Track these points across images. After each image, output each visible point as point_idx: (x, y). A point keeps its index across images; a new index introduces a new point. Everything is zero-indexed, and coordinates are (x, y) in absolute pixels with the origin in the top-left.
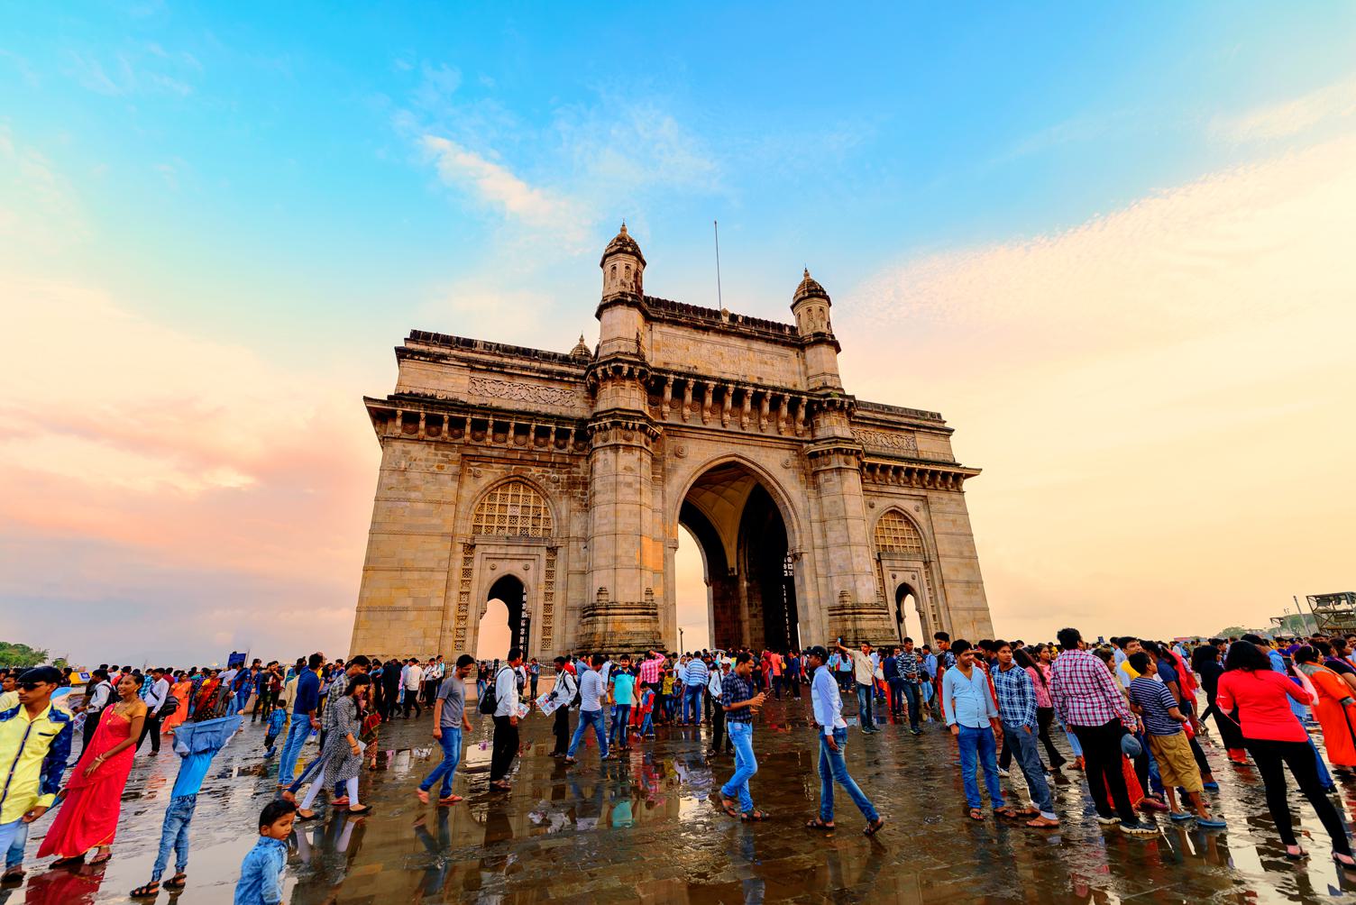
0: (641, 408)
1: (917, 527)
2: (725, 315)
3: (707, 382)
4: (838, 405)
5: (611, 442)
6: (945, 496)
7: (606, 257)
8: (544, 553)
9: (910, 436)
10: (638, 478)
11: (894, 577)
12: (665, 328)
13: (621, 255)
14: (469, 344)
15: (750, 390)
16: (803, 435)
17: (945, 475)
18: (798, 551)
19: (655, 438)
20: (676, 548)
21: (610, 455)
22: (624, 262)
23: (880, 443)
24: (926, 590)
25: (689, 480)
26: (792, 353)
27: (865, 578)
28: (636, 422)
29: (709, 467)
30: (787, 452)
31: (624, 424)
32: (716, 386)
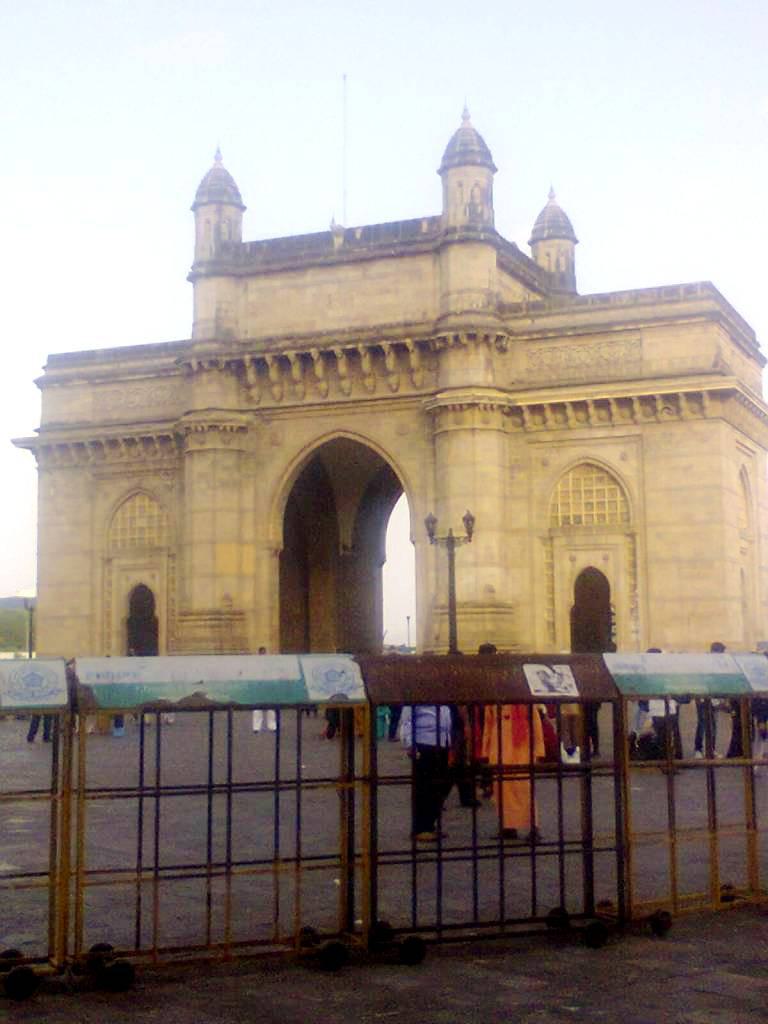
0: (219, 404)
2: (337, 235)
3: (285, 353)
4: (451, 341)
6: (679, 430)
8: (164, 560)
9: (634, 338)
11: (573, 559)
12: (262, 283)
14: (89, 357)
16: (422, 386)
19: (242, 429)
23: (578, 362)
26: (425, 264)
28: (204, 424)
29: (309, 450)
30: (404, 413)
31: (193, 428)
32: (297, 355)
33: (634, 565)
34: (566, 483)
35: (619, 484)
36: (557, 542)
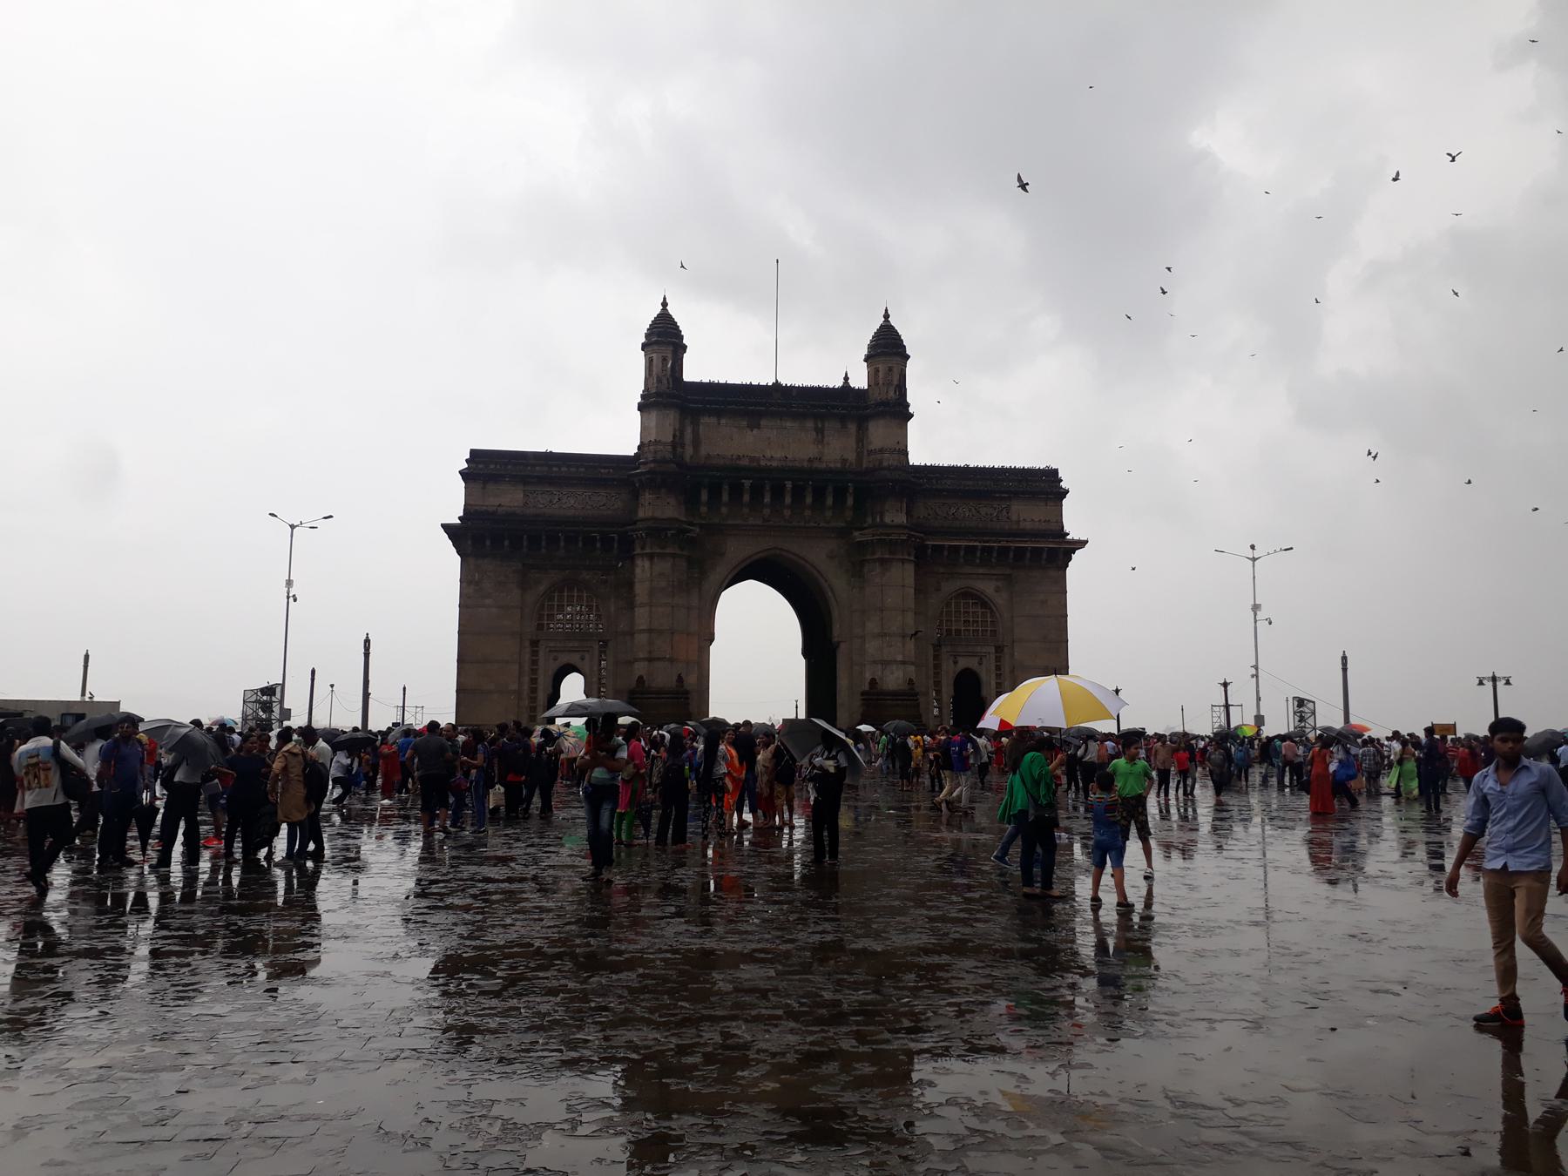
0: (676, 515)
1: (994, 609)
3: (743, 481)
5: (648, 551)
7: (644, 347)
10: (671, 583)
11: (956, 663)
13: (656, 347)
15: (789, 484)
17: (1037, 552)
18: (836, 640)
20: (712, 640)
21: (647, 564)
22: (660, 355)
24: (993, 676)
25: (727, 576)
27: (894, 667)
29: (748, 561)
33: (998, 668)
34: (948, 605)
35: (990, 608)
36: (944, 649)
